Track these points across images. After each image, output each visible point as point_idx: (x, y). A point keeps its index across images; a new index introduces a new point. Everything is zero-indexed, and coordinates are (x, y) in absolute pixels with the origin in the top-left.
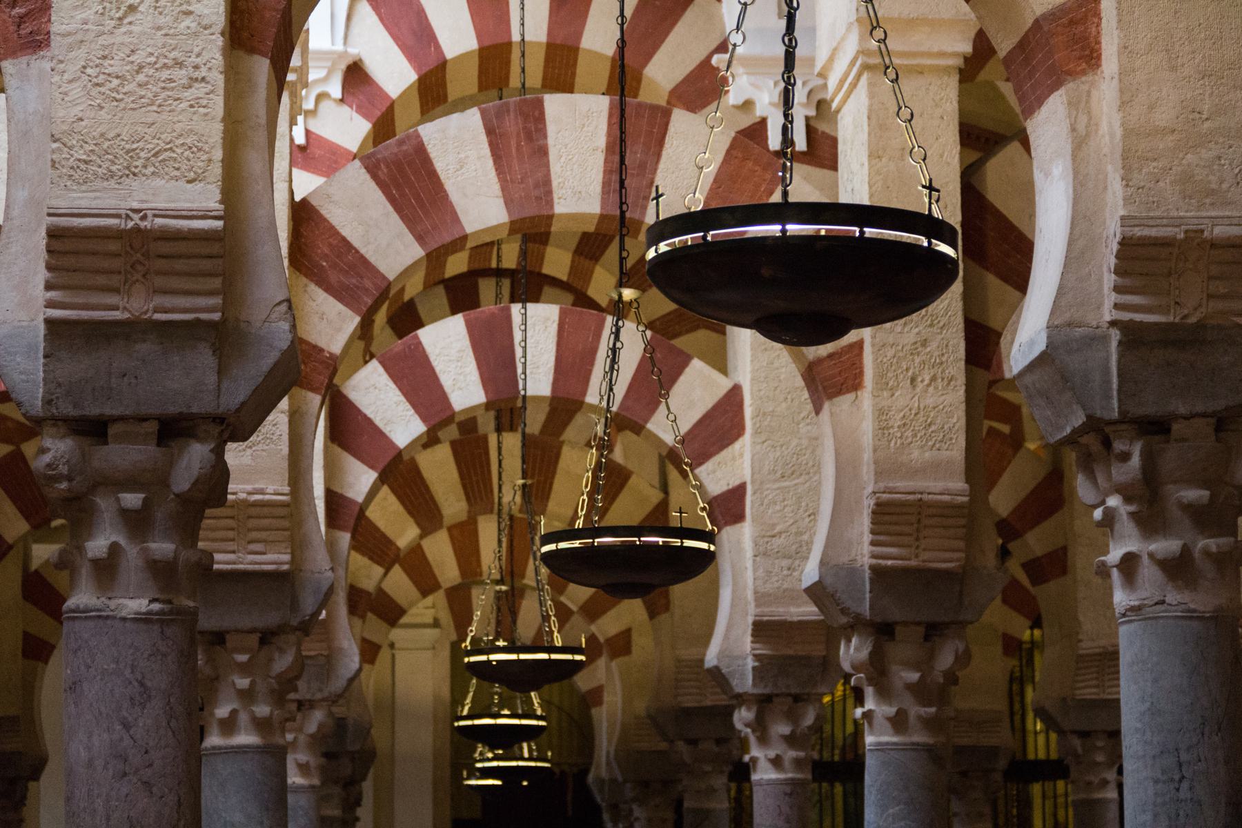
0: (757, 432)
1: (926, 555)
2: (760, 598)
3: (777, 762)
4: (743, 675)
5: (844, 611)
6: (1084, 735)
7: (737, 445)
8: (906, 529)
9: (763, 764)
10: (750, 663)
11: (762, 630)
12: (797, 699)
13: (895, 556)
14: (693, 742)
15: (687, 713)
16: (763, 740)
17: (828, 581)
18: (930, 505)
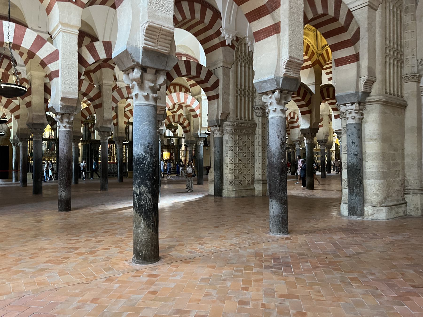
0: (63, 58)
1: (159, 47)
2: (63, 93)
3: (65, 127)
4: (58, 109)
5: (133, 61)
6: (104, 132)
7: (57, 61)
8: (155, 37)
9: (62, 127)
10: (60, 106)
11: (63, 99)
12: (69, 114)
13: (151, 46)
14: (36, 129)
15: (35, 124)
16: (62, 122)
17: (129, 50)
18: (163, 30)
